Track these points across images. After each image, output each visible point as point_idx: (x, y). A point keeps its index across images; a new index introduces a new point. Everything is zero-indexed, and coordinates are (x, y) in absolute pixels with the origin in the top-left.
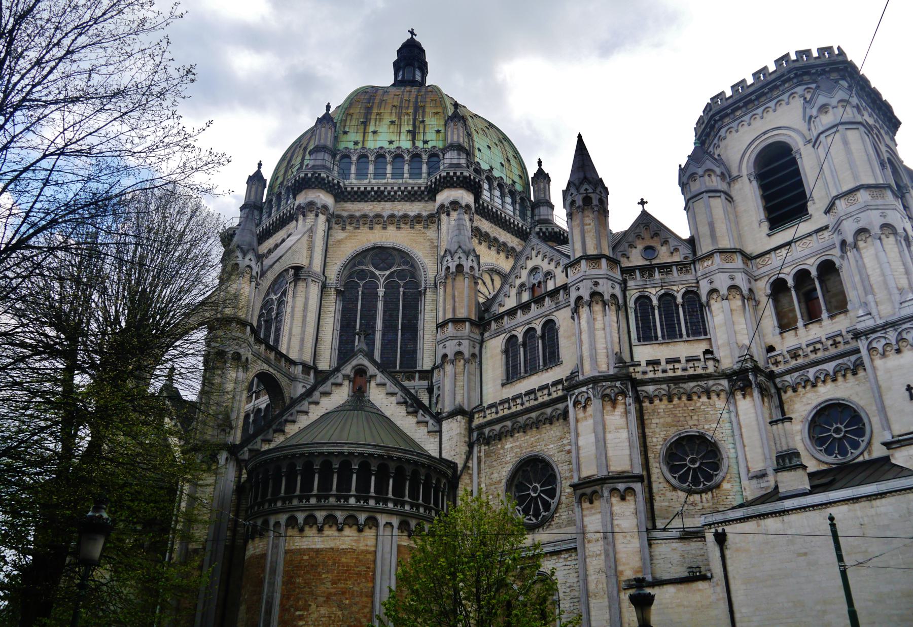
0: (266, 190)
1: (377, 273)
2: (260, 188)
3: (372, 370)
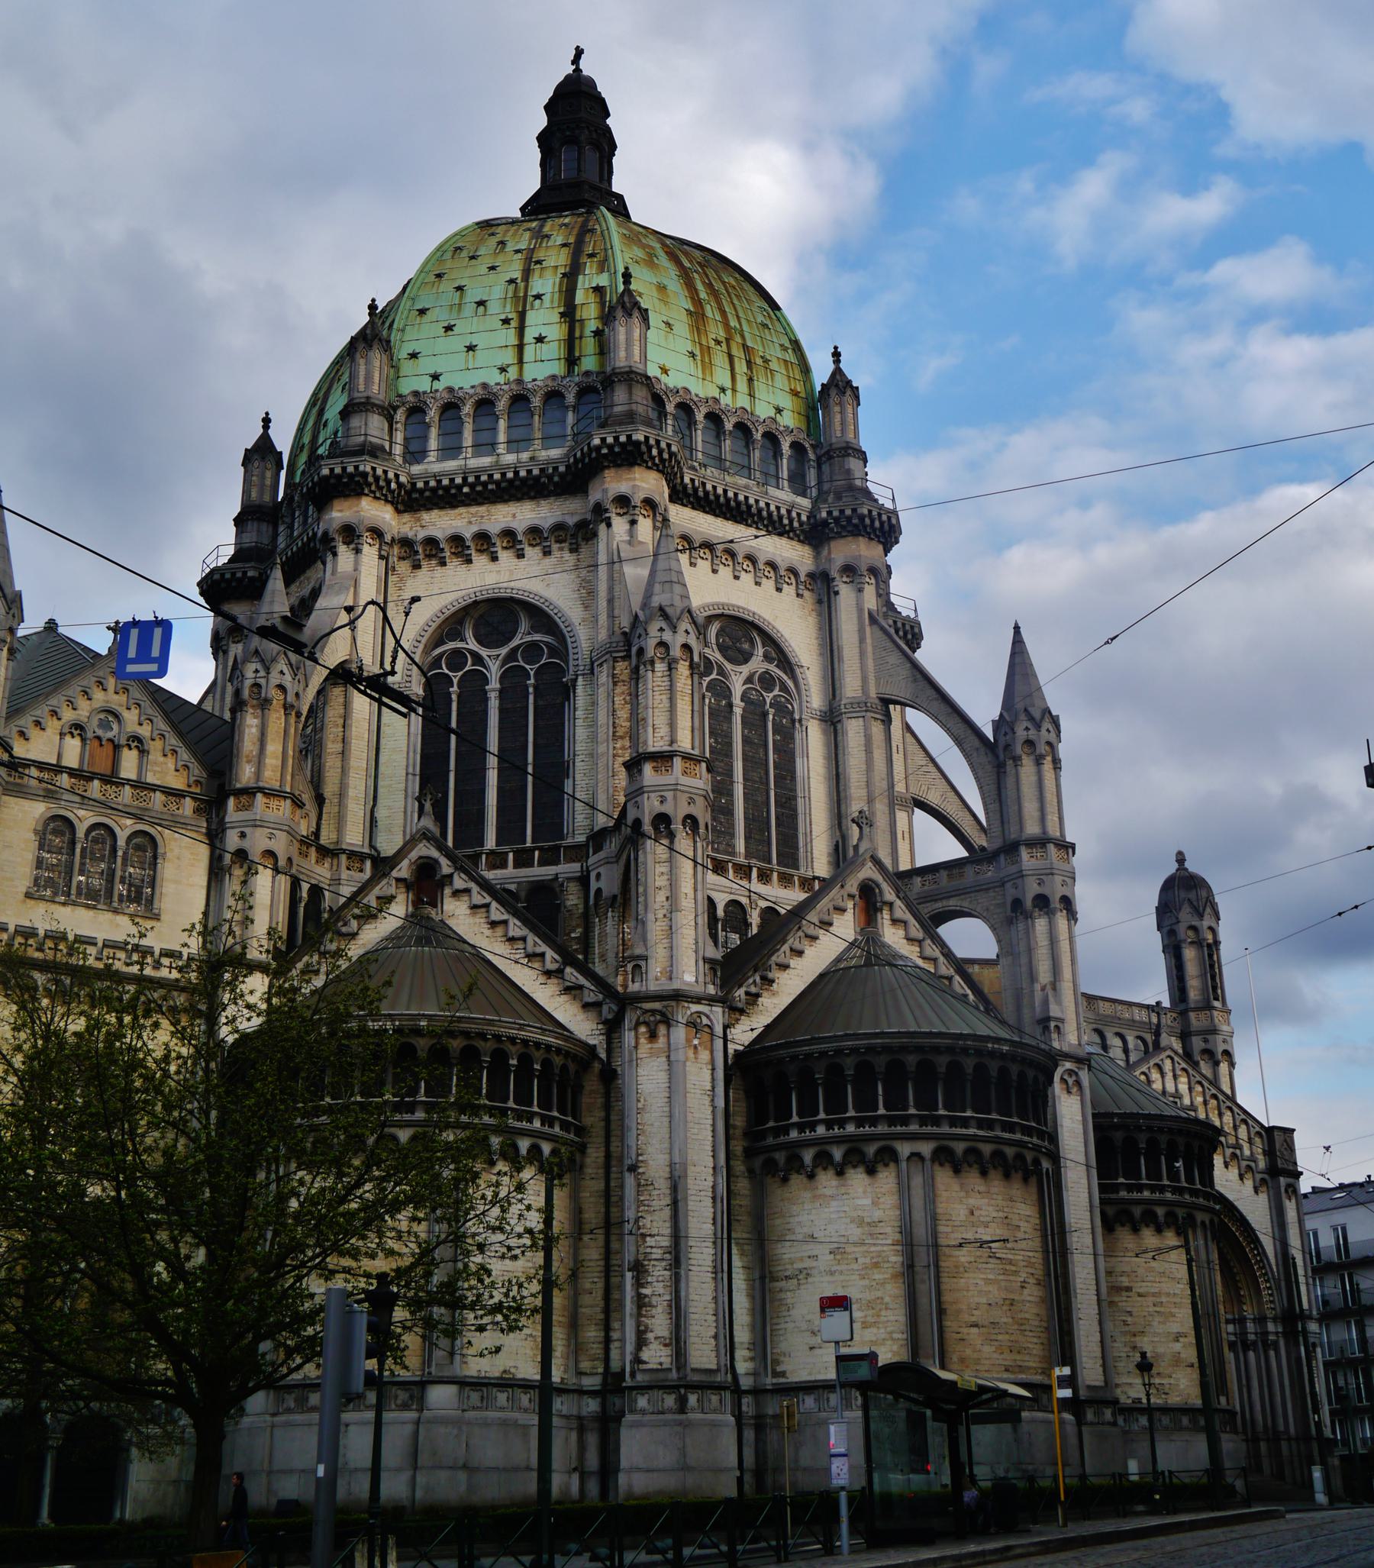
0: (283, 474)
1: (484, 652)
2: (268, 474)
3: (446, 866)
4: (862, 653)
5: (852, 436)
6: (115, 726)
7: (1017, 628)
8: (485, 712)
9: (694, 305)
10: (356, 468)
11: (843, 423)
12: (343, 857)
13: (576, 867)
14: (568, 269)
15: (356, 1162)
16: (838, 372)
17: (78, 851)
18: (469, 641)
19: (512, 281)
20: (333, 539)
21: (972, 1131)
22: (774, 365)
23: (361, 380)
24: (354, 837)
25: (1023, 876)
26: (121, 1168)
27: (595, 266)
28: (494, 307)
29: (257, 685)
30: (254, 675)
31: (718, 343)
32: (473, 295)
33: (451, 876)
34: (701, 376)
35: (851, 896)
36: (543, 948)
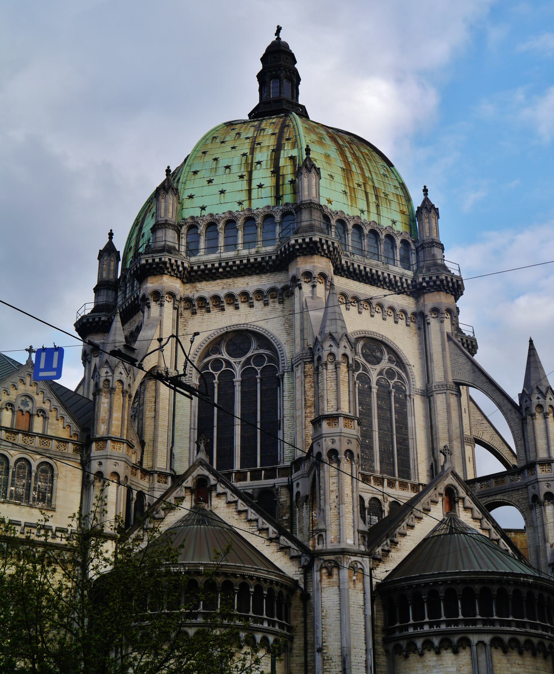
0: (120, 263)
1: (232, 360)
2: (112, 264)
3: (213, 480)
4: (444, 357)
5: (435, 235)
6: (30, 404)
7: (531, 342)
8: (233, 394)
9: (345, 165)
10: (160, 259)
11: (430, 228)
12: (156, 476)
13: (285, 479)
14: (275, 147)
15: (165, 647)
16: (426, 200)
17: (10, 473)
18: (223, 354)
19: (244, 155)
20: (148, 299)
21: (513, 629)
22: (391, 197)
23: (163, 211)
24: (162, 464)
25: (538, 482)
26: (35, 651)
27: (290, 145)
28: (234, 169)
29: (107, 380)
30: (105, 375)
31: (359, 185)
32: (223, 163)
33: (216, 485)
34: (350, 204)
35: (441, 494)
36: (268, 525)
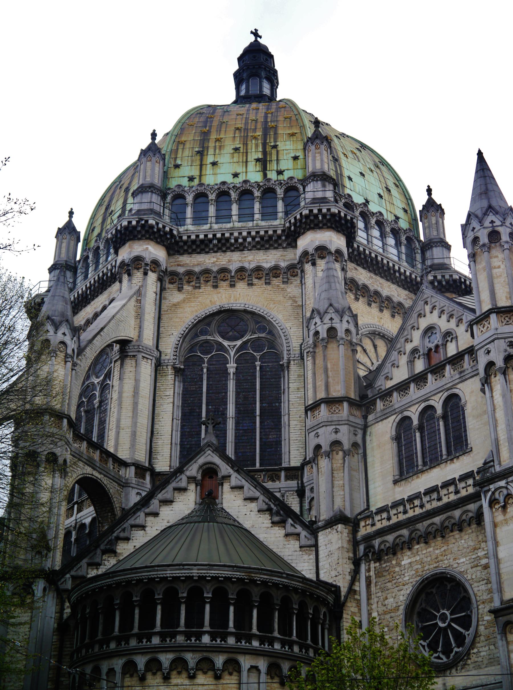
0: (80, 245)
1: (226, 343)
2: (72, 243)
3: (224, 469)
